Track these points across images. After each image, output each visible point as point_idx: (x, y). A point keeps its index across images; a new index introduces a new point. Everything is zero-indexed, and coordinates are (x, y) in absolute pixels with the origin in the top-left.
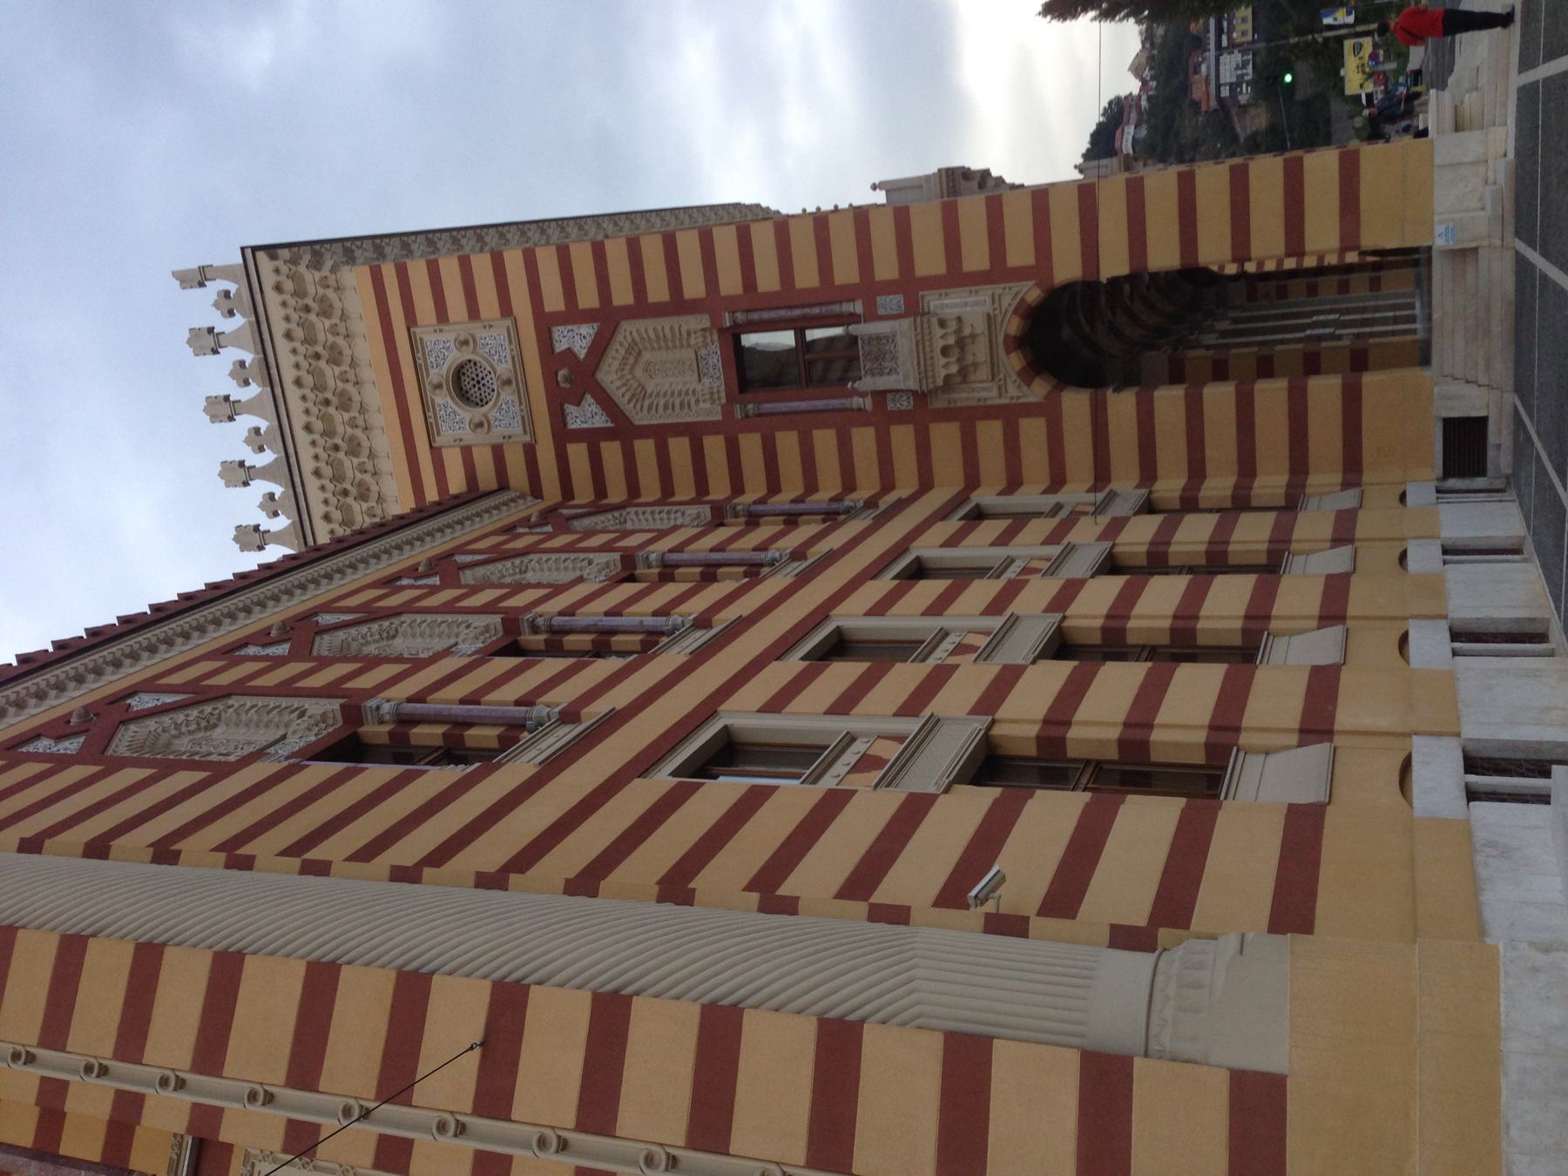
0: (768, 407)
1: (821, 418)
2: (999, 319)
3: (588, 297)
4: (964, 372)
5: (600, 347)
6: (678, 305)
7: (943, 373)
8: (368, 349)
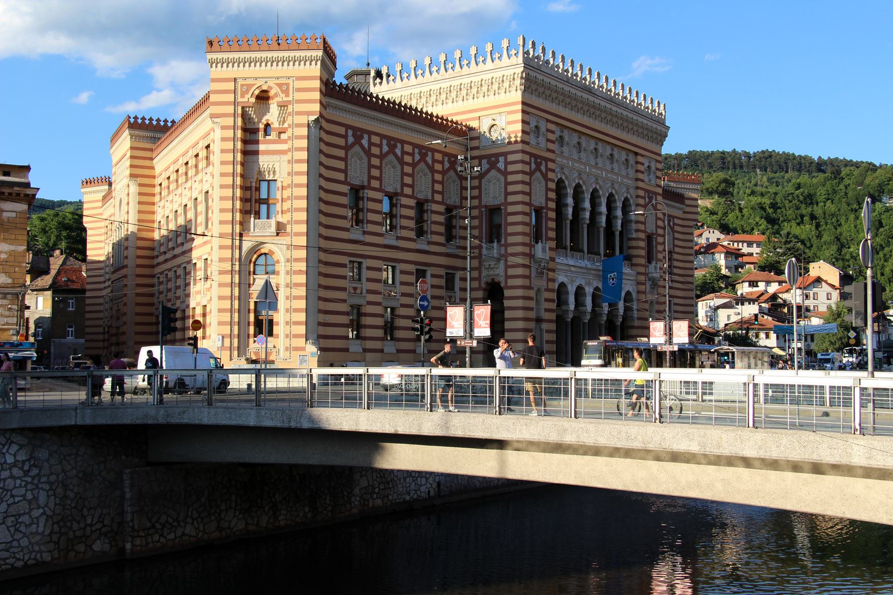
1: (481, 232)
3: (511, 168)
5: (499, 170)
6: (507, 194)
8: (502, 98)
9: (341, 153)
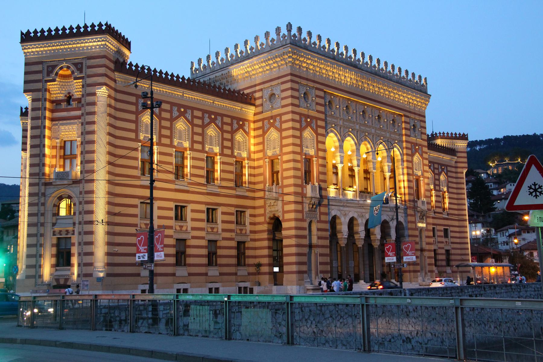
3: (284, 126)
6: (282, 146)
9: (133, 117)
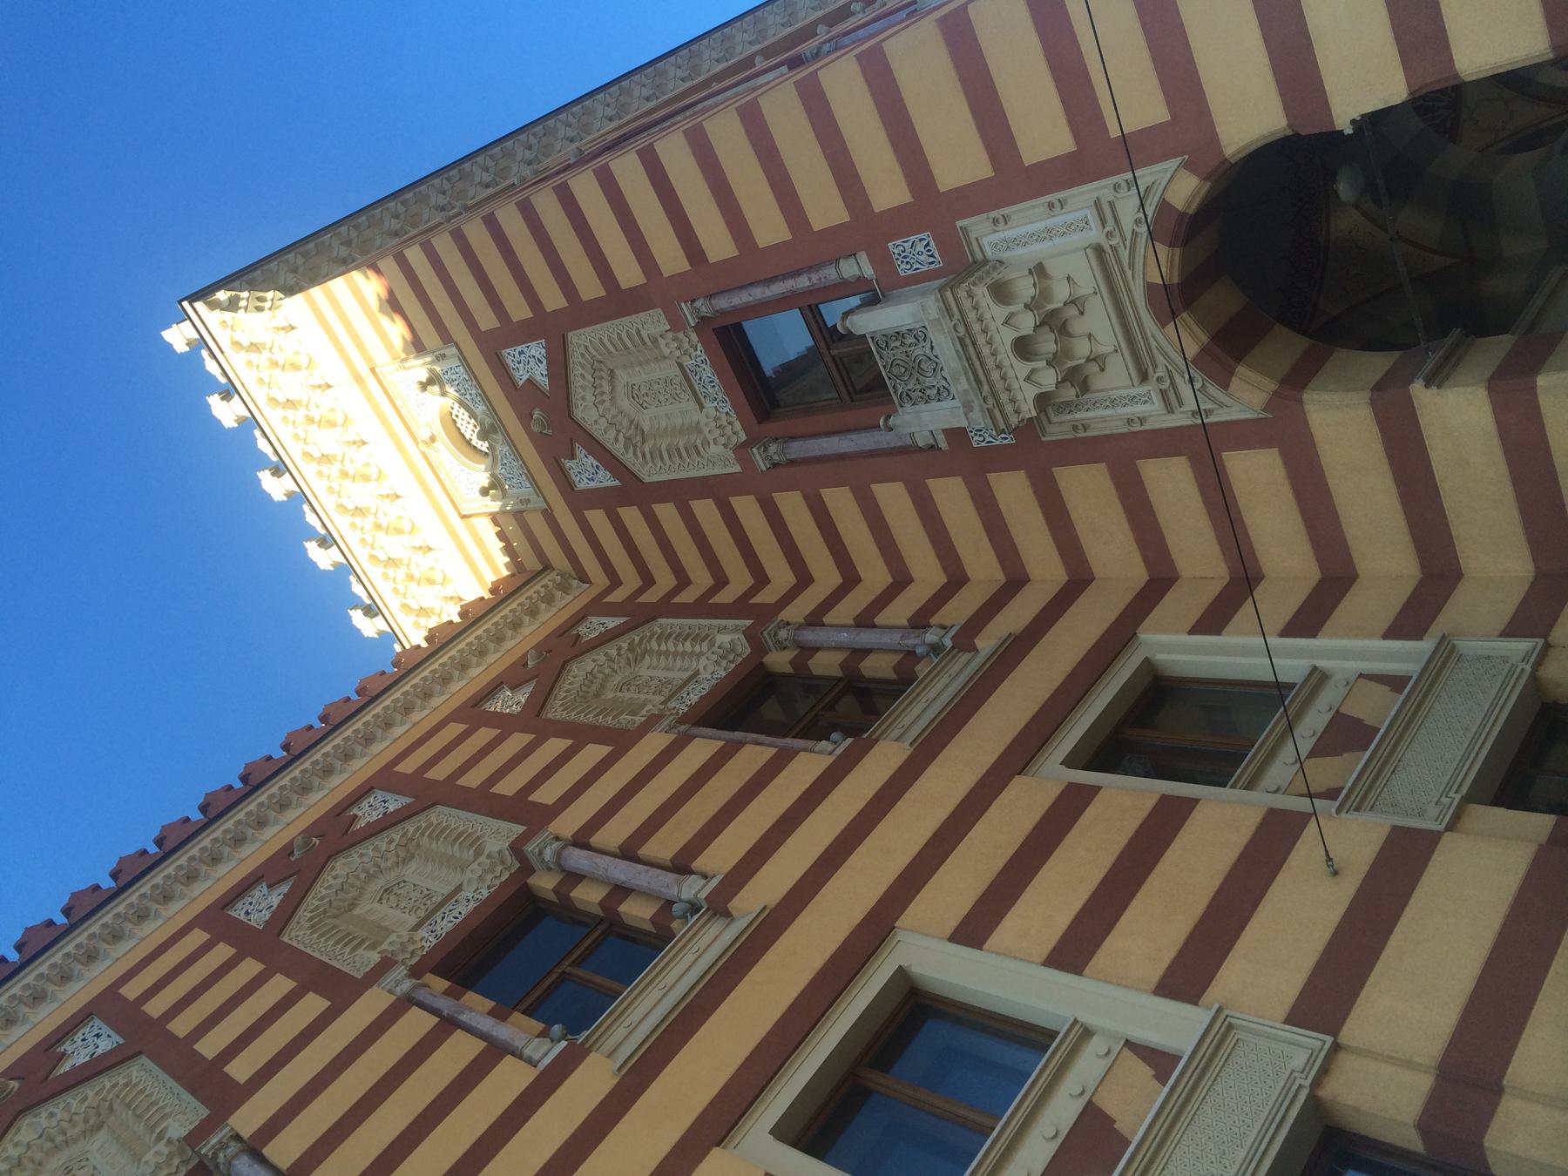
0: (799, 449)
2: (1125, 255)
4: (1077, 378)
6: (619, 302)
7: (1030, 392)
